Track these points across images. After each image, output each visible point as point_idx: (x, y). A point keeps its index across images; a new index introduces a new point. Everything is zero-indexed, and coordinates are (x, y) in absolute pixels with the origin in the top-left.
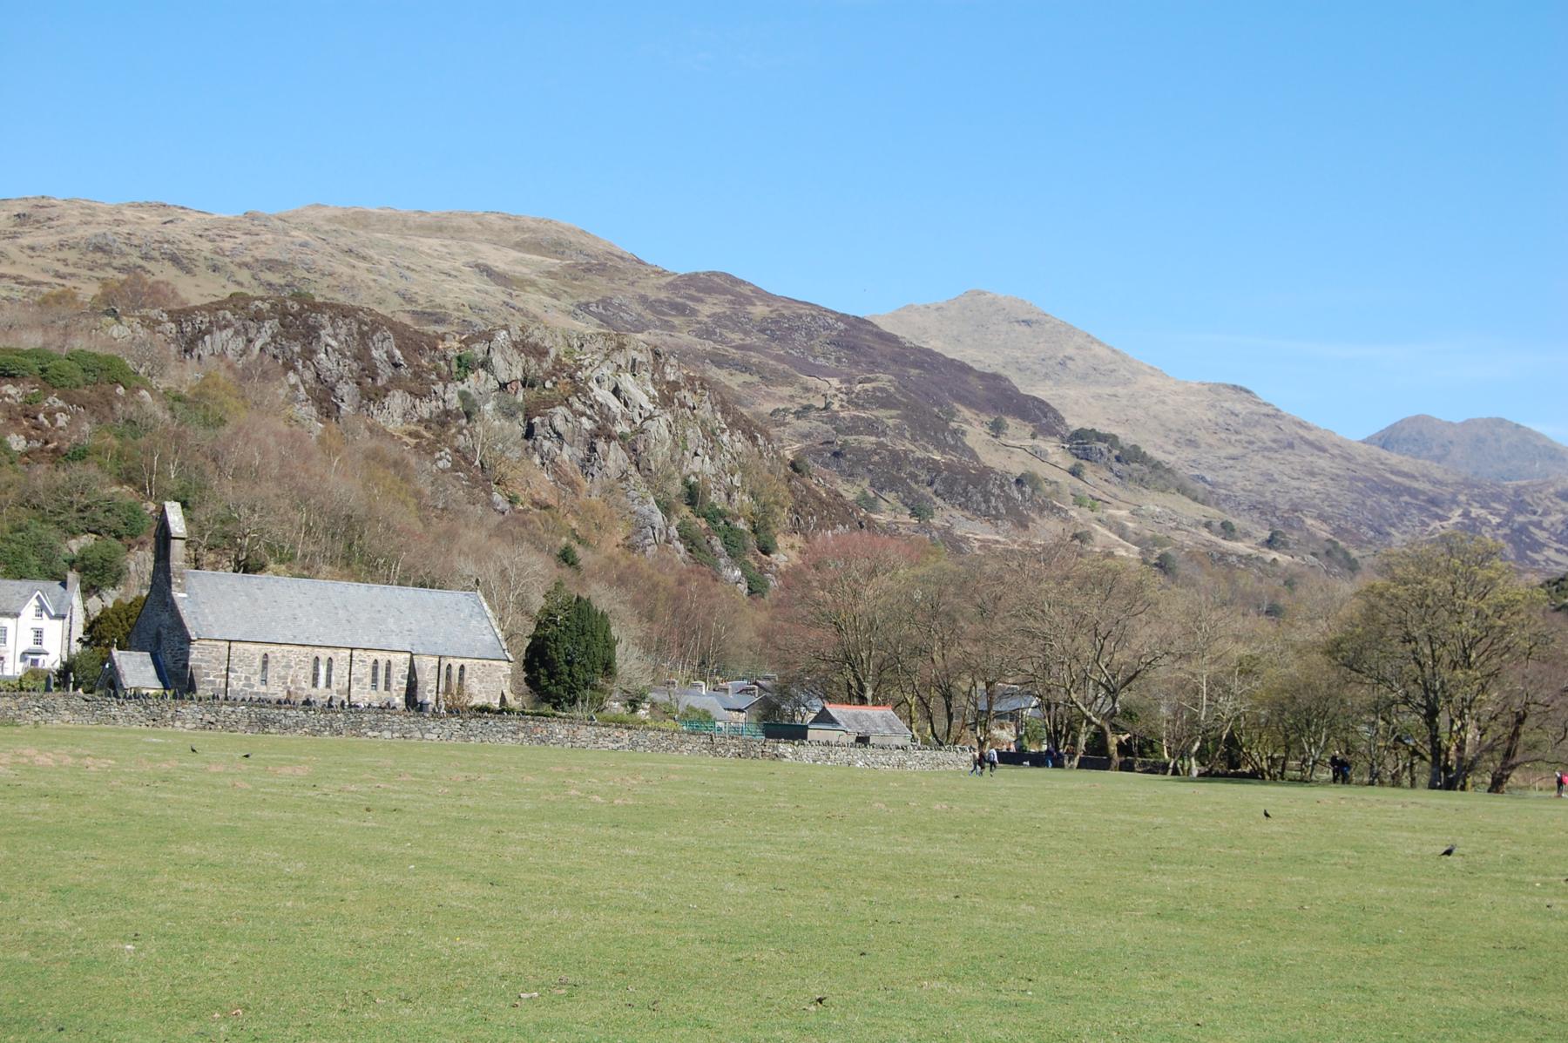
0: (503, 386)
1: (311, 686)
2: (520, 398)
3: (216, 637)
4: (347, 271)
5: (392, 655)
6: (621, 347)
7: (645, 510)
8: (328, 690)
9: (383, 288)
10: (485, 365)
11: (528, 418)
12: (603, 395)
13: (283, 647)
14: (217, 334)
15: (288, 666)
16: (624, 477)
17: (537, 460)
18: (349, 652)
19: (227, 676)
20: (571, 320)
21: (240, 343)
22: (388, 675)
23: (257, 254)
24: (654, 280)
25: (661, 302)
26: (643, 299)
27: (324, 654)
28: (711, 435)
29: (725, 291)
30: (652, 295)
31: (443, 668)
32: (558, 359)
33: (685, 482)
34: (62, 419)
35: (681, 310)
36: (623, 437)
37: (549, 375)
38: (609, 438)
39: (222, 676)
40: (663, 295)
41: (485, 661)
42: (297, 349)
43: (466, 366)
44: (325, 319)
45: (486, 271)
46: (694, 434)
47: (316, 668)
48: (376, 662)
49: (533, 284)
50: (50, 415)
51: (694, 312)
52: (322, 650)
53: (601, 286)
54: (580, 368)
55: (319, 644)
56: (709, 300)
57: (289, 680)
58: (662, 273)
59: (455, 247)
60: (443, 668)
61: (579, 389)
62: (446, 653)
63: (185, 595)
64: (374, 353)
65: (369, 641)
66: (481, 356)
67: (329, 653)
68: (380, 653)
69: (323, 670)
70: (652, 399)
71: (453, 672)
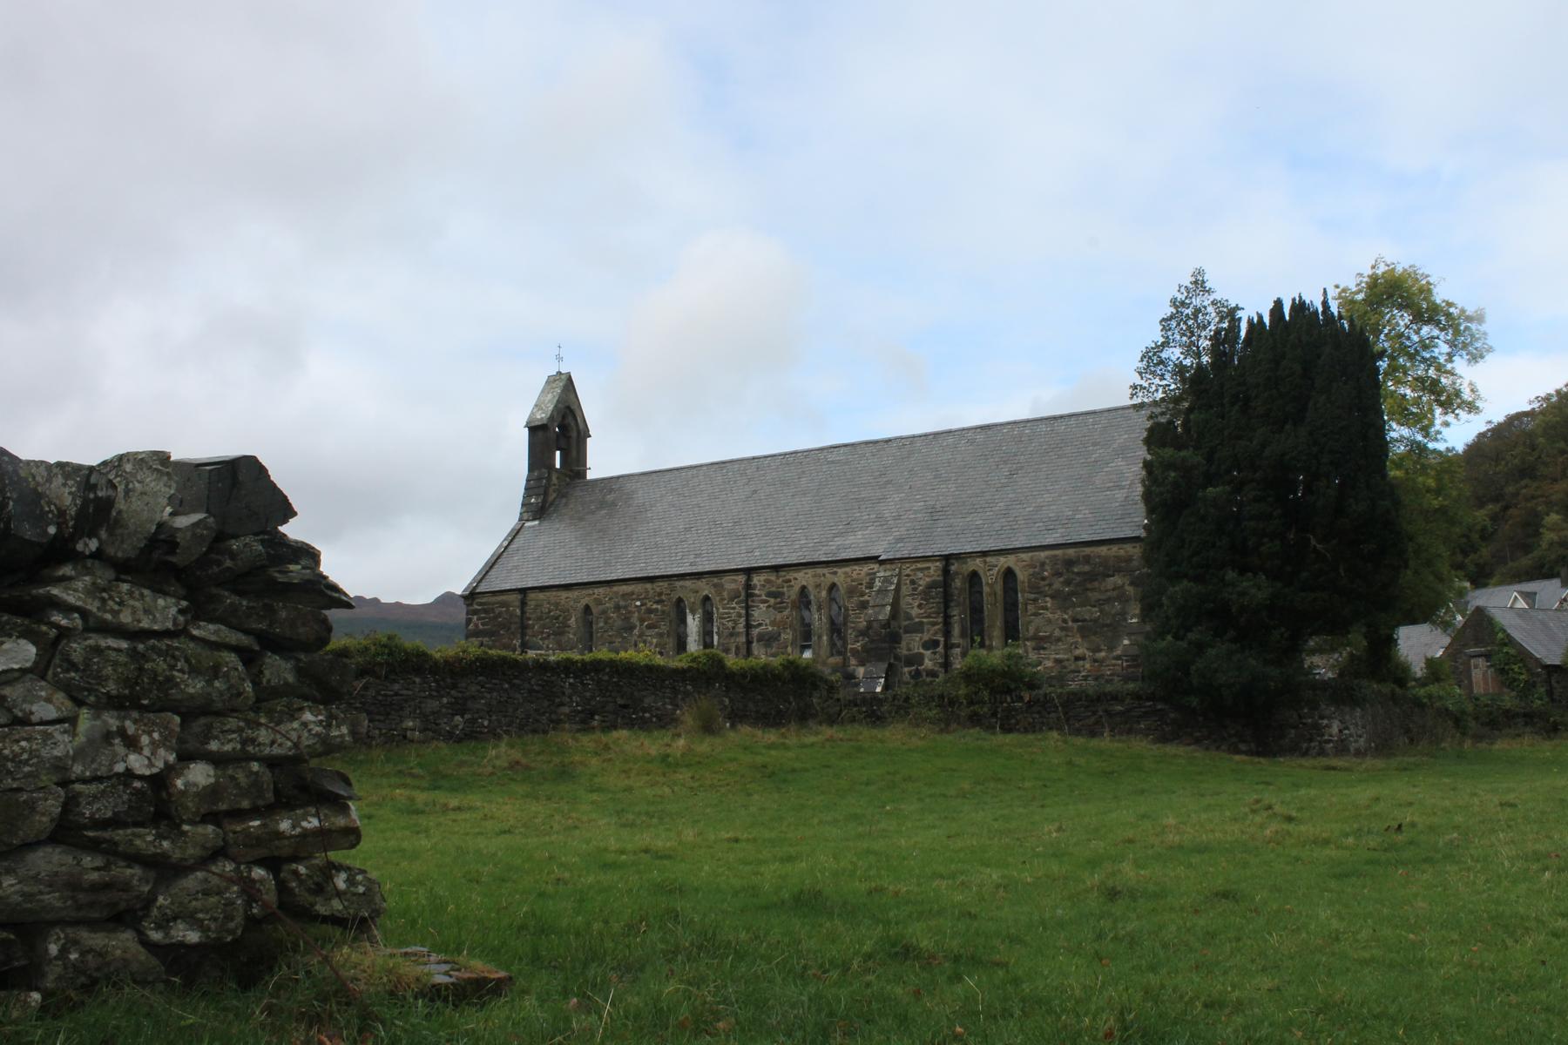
5: (840, 571)
18: (742, 578)
31: (958, 583)
41: (1071, 552)
52: (688, 583)
67: (705, 588)
68: (810, 572)
69: (693, 624)
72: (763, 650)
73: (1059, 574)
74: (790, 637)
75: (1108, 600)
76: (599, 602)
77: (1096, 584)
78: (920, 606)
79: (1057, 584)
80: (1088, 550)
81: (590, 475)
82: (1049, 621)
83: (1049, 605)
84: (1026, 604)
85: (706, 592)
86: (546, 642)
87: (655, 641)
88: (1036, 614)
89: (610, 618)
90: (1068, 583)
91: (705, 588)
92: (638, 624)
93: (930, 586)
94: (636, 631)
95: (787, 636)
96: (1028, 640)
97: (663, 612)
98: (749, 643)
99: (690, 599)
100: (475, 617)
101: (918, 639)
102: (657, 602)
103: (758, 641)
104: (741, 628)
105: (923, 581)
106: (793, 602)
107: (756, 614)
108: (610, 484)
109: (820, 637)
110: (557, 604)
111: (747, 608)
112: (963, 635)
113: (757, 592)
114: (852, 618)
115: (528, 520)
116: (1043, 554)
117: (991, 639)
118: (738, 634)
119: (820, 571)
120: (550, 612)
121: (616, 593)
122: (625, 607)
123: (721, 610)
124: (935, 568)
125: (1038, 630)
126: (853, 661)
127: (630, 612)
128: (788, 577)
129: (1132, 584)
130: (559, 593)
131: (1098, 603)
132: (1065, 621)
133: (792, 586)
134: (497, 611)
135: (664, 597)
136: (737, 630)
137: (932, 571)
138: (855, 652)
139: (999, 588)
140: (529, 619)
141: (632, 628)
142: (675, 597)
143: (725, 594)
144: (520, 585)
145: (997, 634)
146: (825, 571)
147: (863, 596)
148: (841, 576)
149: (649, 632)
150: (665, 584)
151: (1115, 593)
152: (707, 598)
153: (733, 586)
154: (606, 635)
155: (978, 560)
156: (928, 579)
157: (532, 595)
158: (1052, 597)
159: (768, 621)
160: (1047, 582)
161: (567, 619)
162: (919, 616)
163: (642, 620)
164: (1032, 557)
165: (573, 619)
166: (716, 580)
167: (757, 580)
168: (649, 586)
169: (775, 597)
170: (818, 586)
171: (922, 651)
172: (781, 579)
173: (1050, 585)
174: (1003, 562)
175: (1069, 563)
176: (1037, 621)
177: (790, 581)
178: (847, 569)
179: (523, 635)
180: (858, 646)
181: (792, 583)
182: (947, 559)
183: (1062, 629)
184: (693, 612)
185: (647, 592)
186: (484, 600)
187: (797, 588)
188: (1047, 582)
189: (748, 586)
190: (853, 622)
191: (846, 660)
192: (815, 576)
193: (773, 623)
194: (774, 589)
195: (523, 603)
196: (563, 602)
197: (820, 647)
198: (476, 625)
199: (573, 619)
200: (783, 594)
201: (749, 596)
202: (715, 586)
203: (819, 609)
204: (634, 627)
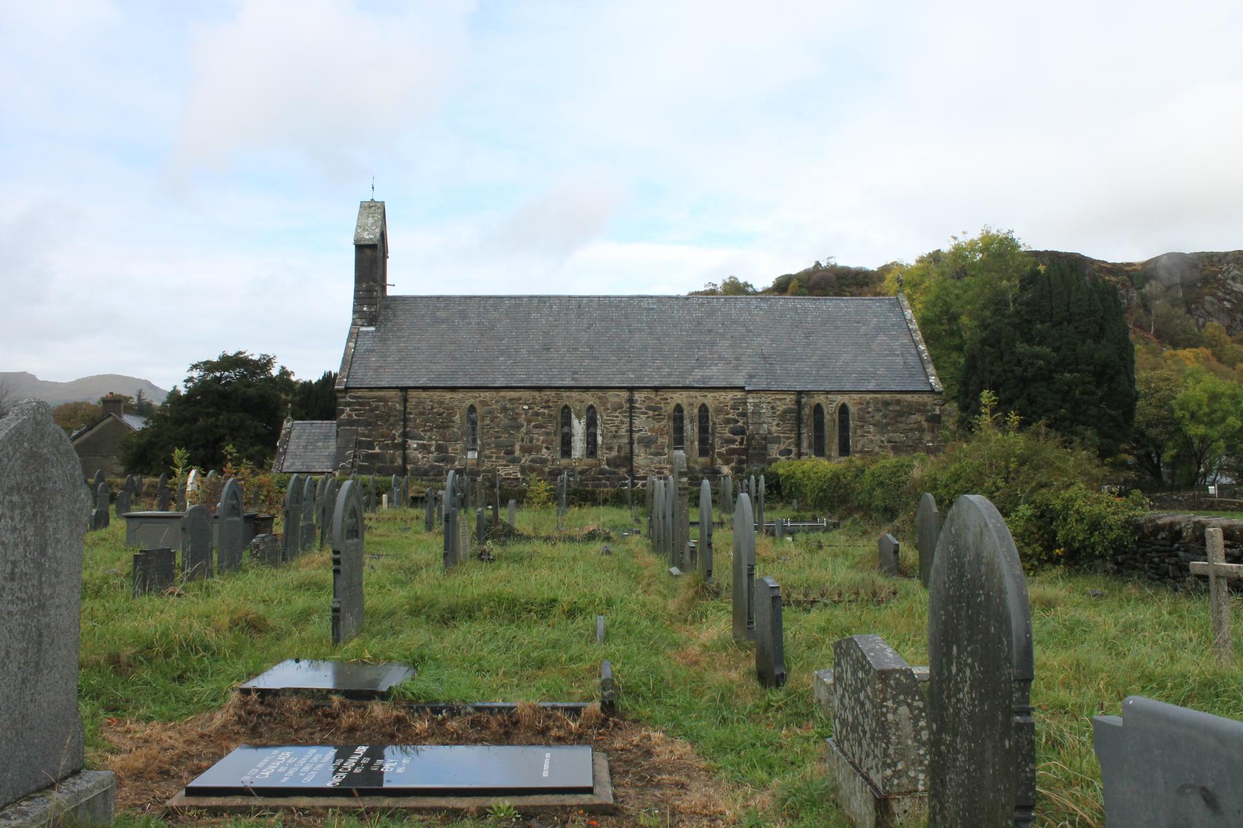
1: (558, 455)
3: (384, 384)
5: (710, 395)
8: (591, 461)
13: (502, 394)
18: (625, 394)
19: (404, 446)
22: (703, 430)
31: (806, 411)
39: (395, 446)
41: (887, 396)
47: (567, 422)
48: (679, 408)
52: (575, 394)
55: (572, 383)
57: (517, 447)
62: (810, 387)
63: (372, 329)
65: (670, 375)
67: (590, 399)
68: (685, 393)
69: (578, 427)
71: (827, 417)
72: (643, 450)
73: (878, 410)
74: (667, 441)
75: (911, 430)
76: (484, 403)
77: (903, 419)
78: (778, 425)
79: (878, 417)
80: (898, 396)
81: (390, 292)
82: (872, 441)
83: (872, 430)
84: (856, 429)
85: (591, 403)
86: (428, 434)
87: (542, 438)
88: (862, 436)
89: (497, 417)
90: (885, 416)
91: (590, 399)
92: (525, 423)
93: (785, 412)
94: (523, 430)
95: (664, 440)
96: (856, 452)
97: (550, 416)
98: (631, 443)
99: (575, 407)
100: (348, 409)
101: (776, 448)
102: (544, 408)
103: (639, 443)
104: (623, 431)
105: (781, 408)
106: (669, 416)
107: (637, 422)
108: (394, 298)
109: (692, 442)
110: (441, 403)
111: (631, 417)
112: (810, 446)
113: (637, 405)
114: (718, 430)
115: (362, 326)
116: (868, 396)
117: (830, 450)
118: (621, 437)
119: (693, 393)
120: (432, 408)
121: (504, 397)
122: (513, 410)
123: (605, 417)
124: (790, 399)
125: (863, 446)
126: (719, 461)
127: (518, 414)
128: (665, 396)
129: (926, 420)
130: (443, 394)
131: (904, 431)
132: (882, 442)
133: (668, 403)
134: (374, 405)
135: (550, 404)
136: (619, 433)
137: (787, 401)
138: (720, 455)
139: (836, 417)
140: (411, 413)
141: (519, 427)
142: (562, 404)
143: (609, 405)
144: (401, 384)
145: (833, 446)
146: (698, 394)
147: (727, 414)
148: (710, 399)
149: (536, 431)
150: (552, 393)
151: (916, 426)
152: (591, 407)
153: (617, 399)
154: (491, 431)
155: (822, 397)
156: (784, 407)
157: (412, 394)
158: (874, 425)
159: (647, 428)
160: (870, 415)
161: (451, 415)
162: (776, 432)
163: (529, 422)
164: (861, 398)
165: (458, 416)
166: (600, 394)
167: (638, 396)
168: (536, 394)
169: (654, 411)
170: (691, 405)
171: (778, 456)
172: (659, 397)
173: (873, 417)
174: (840, 399)
175: (886, 404)
176: (863, 441)
177: (667, 399)
178: (716, 394)
179: (405, 426)
180: (723, 450)
181: (669, 401)
182: (800, 393)
183: (880, 447)
184: (579, 417)
185: (534, 398)
186: (359, 394)
187: (673, 405)
188: (870, 415)
189: (631, 401)
190: (719, 433)
191: (713, 460)
192: (687, 397)
193: (651, 430)
194: (653, 404)
195: (405, 400)
196: (447, 401)
197: (692, 449)
198: (350, 416)
199: (458, 416)
200: (661, 408)
201: (632, 408)
202: (600, 398)
203: (692, 421)
204: (522, 426)
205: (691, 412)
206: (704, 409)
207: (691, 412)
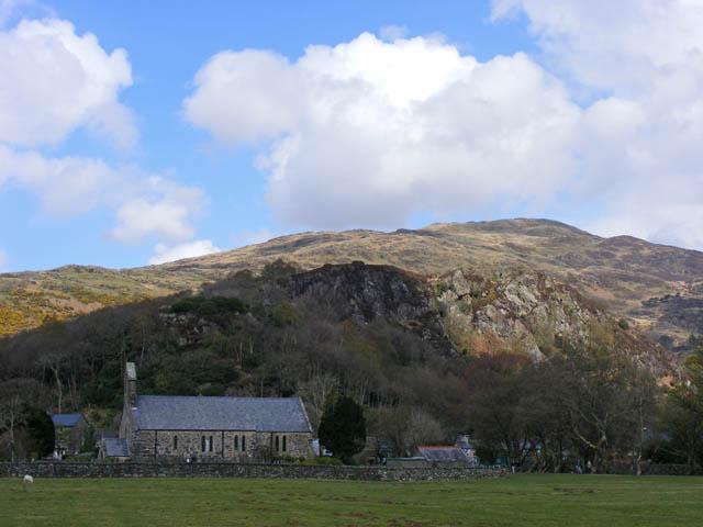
0: (460, 297)
2: (469, 303)
4: (443, 252)
6: (521, 273)
7: (533, 352)
9: (460, 259)
10: (451, 288)
11: (474, 312)
12: (512, 297)
14: (315, 285)
15: (189, 441)
16: (523, 337)
17: (480, 332)
20: (552, 266)
21: (326, 287)
23: (401, 248)
24: (594, 243)
25: (597, 253)
26: (588, 252)
27: (240, 435)
28: (569, 313)
29: (629, 245)
30: (592, 250)
32: (489, 281)
33: (556, 336)
34: (205, 329)
35: (607, 255)
36: (523, 317)
37: (484, 290)
38: (515, 318)
40: (598, 250)
42: (354, 288)
43: (443, 289)
44: (366, 273)
45: (511, 246)
46: (560, 312)
49: (534, 250)
50: (200, 328)
51: (614, 256)
53: (567, 248)
54: (499, 285)
56: (621, 249)
58: (598, 238)
59: (498, 236)
60: (274, 439)
61: (500, 295)
64: (393, 287)
66: (448, 284)
67: (211, 434)
69: (207, 442)
70: (537, 297)
148: (246, 434)
205: (240, 438)
206: (244, 437)
207: (240, 438)
